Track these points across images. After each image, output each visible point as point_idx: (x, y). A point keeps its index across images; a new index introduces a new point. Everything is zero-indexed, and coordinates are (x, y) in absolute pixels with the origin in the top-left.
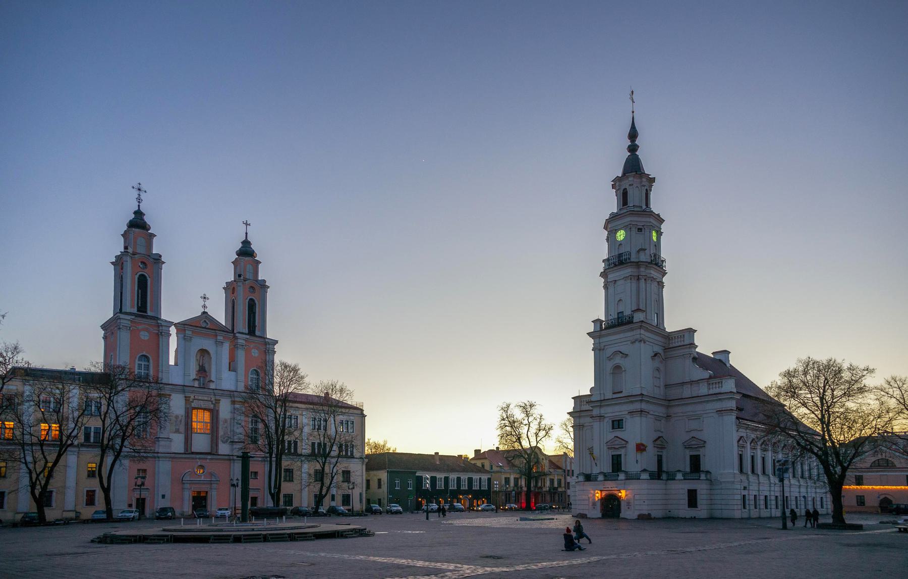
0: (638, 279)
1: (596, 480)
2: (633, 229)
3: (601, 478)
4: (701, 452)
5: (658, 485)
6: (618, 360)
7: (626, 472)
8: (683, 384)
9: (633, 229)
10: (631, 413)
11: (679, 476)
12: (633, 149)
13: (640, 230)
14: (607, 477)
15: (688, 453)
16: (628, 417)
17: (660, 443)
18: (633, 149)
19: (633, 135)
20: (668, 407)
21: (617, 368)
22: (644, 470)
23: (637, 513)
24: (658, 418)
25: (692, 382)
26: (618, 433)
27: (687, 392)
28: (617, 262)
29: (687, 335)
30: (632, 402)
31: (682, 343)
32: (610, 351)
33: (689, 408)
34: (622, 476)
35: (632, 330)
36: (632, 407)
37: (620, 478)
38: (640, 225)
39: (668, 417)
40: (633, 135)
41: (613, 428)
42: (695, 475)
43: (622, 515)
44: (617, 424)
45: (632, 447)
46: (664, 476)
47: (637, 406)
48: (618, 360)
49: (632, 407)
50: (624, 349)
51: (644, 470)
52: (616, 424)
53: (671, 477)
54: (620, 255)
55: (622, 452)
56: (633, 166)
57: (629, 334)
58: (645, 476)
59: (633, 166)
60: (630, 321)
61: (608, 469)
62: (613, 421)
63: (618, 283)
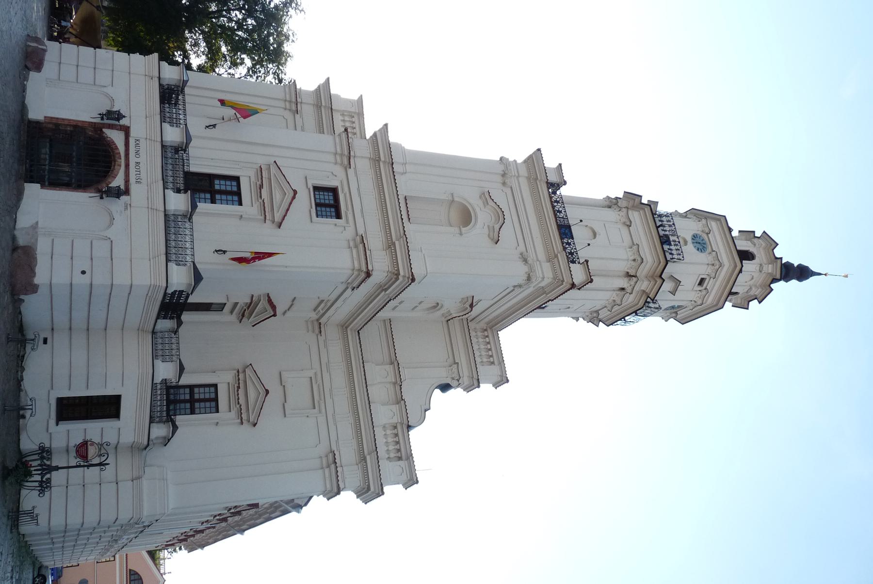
0: (628, 275)
1: (163, 120)
2: (710, 270)
3: (173, 135)
4: (226, 413)
5: (142, 310)
6: (483, 217)
7: (189, 216)
8: (394, 362)
9: (710, 270)
11: (166, 371)
13: (702, 282)
14: (174, 153)
15: (224, 380)
16: (349, 233)
17: (257, 310)
19: (802, 273)
20: (344, 327)
21: (466, 217)
22: (198, 277)
24: (323, 307)
25: (398, 384)
26: (304, 202)
27: (379, 377)
28: (663, 231)
29: (495, 369)
30: (390, 246)
31: (478, 360)
32: (501, 197)
33: (338, 378)
34: (178, 202)
35: (551, 258)
36: (376, 242)
37: (170, 193)
38: (709, 284)
39: (319, 326)
40: (802, 273)
41: (316, 189)
42: (161, 405)
43: (32, 190)
44: (328, 202)
45: (262, 237)
46: (166, 324)
47: (380, 265)
48: (483, 217)
49: (376, 242)
51: (198, 277)
52: (329, 198)
53: (162, 346)
55: (249, 206)
58: (180, 278)
60: (572, 258)
61: (203, 159)
62: (334, 191)
63: (625, 230)
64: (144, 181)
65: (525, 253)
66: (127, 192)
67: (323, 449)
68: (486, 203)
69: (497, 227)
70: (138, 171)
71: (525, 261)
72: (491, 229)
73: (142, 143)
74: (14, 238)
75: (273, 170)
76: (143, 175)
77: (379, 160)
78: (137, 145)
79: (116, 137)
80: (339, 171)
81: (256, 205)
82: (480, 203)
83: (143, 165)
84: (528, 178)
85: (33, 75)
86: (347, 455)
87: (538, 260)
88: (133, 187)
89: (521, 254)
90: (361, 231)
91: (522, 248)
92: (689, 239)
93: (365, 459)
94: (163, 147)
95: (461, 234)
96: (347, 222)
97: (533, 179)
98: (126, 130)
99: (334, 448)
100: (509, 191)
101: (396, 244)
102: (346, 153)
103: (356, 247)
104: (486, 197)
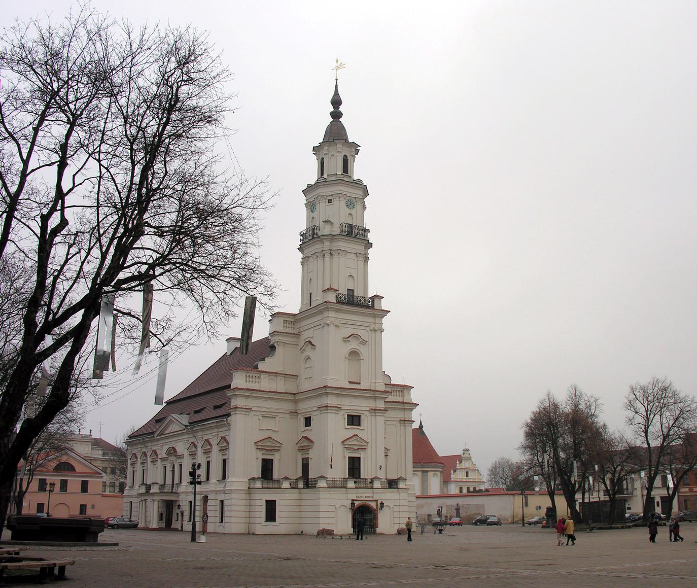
6: (354, 345)
10: (374, 411)
12: (336, 115)
18: (336, 115)
19: (336, 102)
21: (354, 354)
23: (397, 527)
26: (354, 430)
30: (375, 398)
32: (347, 332)
34: (377, 484)
36: (372, 404)
40: (336, 102)
43: (378, 530)
44: (354, 420)
50: (364, 334)
54: (351, 226)
56: (336, 133)
57: (371, 320)
59: (336, 133)
62: (348, 415)
63: (349, 255)
64: (372, 495)
65: (371, 328)
66: (376, 501)
67: (397, 424)
68: (349, 341)
69: (361, 340)
70: (368, 497)
71: (375, 331)
72: (361, 343)
73: (357, 495)
74: (395, 534)
75: (346, 443)
76: (370, 495)
77: (339, 394)
78: (358, 497)
79: (357, 503)
80: (341, 413)
81: (360, 451)
82: (348, 344)
83: (364, 496)
84: (336, 312)
85: (335, 533)
86: (400, 415)
87: (375, 323)
88: (375, 498)
89: (371, 330)
90: (368, 409)
91: (368, 329)
92: (348, 211)
93: (404, 408)
94: (356, 488)
95: (363, 359)
96: (363, 414)
97: (338, 311)
98: (353, 500)
99: (398, 420)
100: (341, 325)
101: (373, 393)
102: (336, 409)
103: (375, 413)
104: (346, 339)
